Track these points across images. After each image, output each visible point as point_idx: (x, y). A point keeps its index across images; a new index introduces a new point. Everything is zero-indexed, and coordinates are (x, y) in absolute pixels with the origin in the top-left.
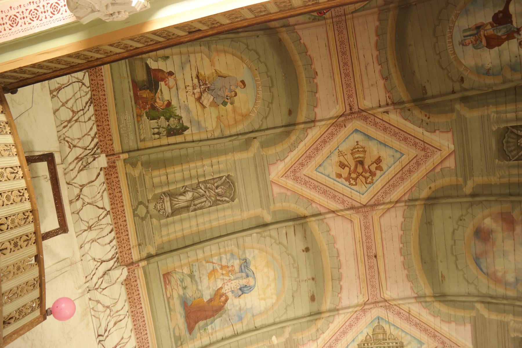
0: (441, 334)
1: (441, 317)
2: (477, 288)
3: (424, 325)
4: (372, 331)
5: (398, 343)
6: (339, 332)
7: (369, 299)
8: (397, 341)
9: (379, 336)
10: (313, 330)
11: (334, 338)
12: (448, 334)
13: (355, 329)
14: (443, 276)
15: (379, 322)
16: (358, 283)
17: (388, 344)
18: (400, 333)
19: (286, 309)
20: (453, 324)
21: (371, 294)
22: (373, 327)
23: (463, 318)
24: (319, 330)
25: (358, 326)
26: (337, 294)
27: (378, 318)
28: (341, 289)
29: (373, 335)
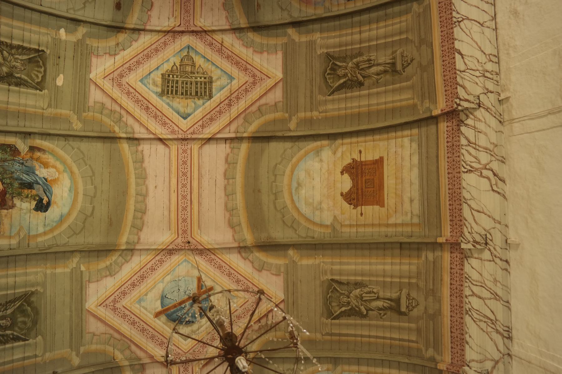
0: (252, 66)
1: (253, 48)
2: (290, 13)
3: (236, 57)
4: (180, 61)
5: (207, 78)
6: (142, 54)
7: (180, 24)
8: (205, 76)
9: (187, 67)
10: (112, 42)
11: (135, 60)
12: (259, 66)
13: (161, 55)
14: (259, 5)
15: (188, 52)
16: (171, 4)
17: (196, 78)
18: (210, 66)
19: (84, 4)
20: (265, 54)
21: (184, 18)
22: (182, 57)
23: (276, 45)
24: (120, 45)
25: (165, 52)
26: (146, 10)
27: (188, 47)
28: (152, 6)
29: (180, 65)
